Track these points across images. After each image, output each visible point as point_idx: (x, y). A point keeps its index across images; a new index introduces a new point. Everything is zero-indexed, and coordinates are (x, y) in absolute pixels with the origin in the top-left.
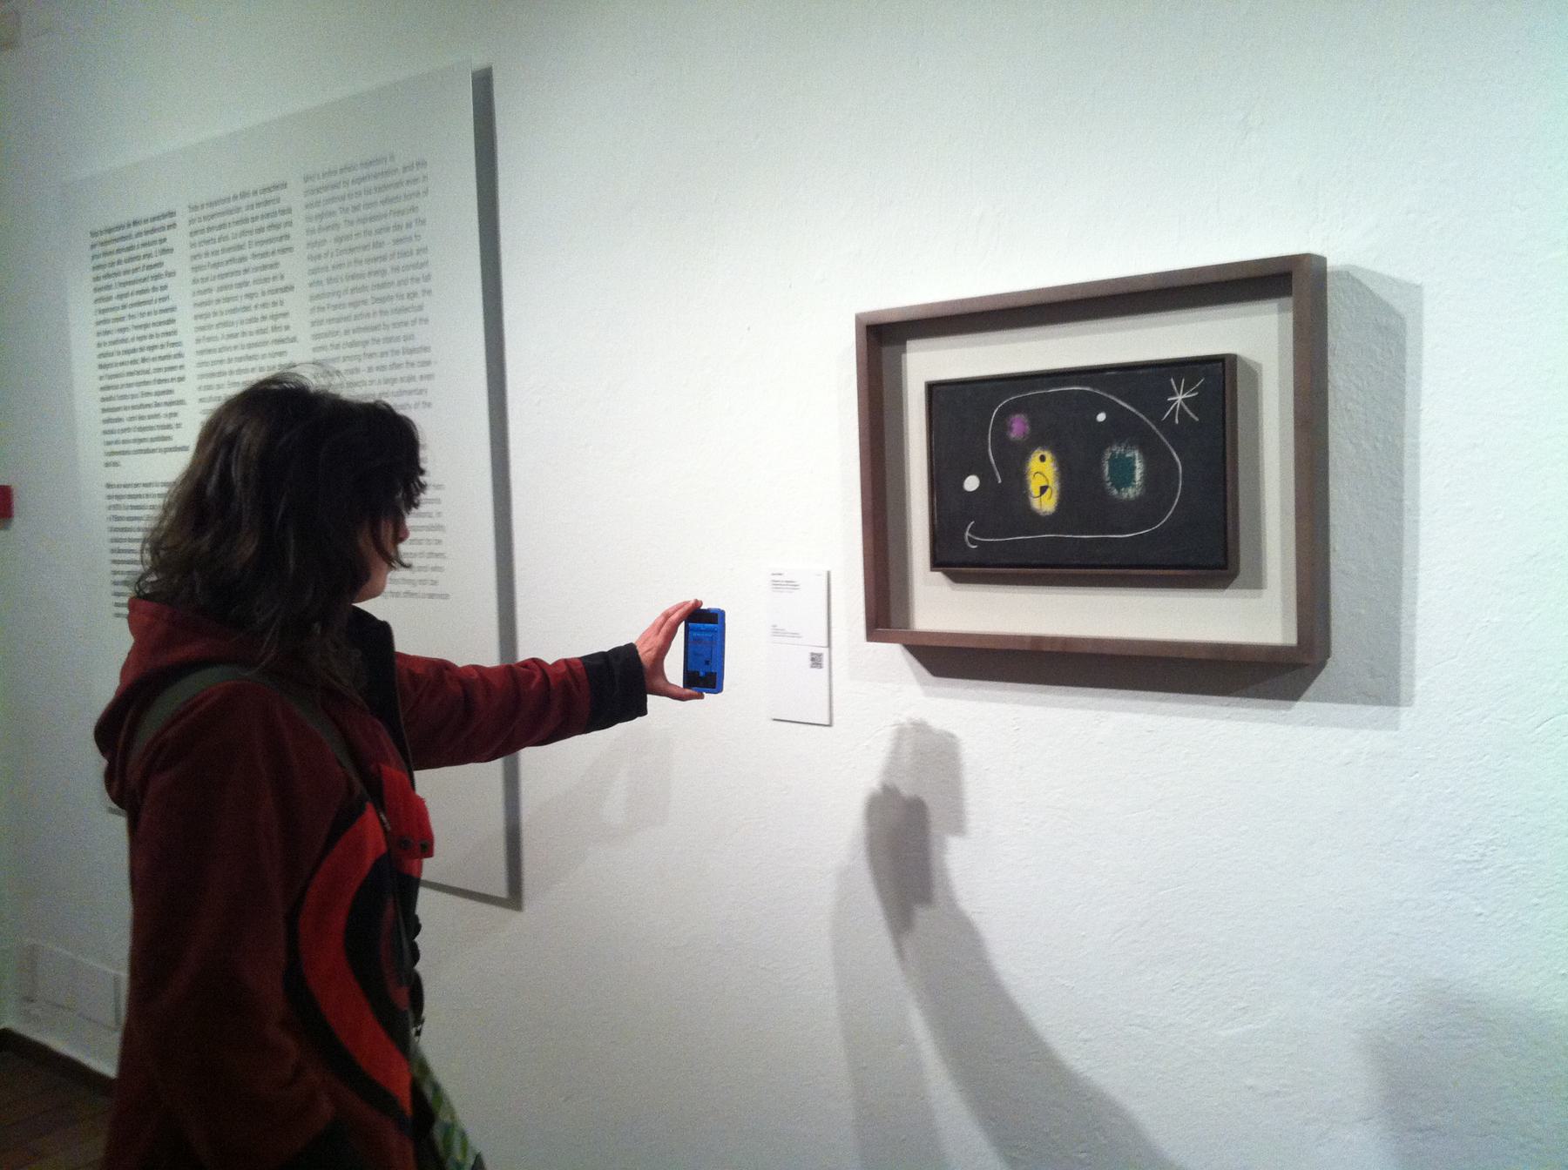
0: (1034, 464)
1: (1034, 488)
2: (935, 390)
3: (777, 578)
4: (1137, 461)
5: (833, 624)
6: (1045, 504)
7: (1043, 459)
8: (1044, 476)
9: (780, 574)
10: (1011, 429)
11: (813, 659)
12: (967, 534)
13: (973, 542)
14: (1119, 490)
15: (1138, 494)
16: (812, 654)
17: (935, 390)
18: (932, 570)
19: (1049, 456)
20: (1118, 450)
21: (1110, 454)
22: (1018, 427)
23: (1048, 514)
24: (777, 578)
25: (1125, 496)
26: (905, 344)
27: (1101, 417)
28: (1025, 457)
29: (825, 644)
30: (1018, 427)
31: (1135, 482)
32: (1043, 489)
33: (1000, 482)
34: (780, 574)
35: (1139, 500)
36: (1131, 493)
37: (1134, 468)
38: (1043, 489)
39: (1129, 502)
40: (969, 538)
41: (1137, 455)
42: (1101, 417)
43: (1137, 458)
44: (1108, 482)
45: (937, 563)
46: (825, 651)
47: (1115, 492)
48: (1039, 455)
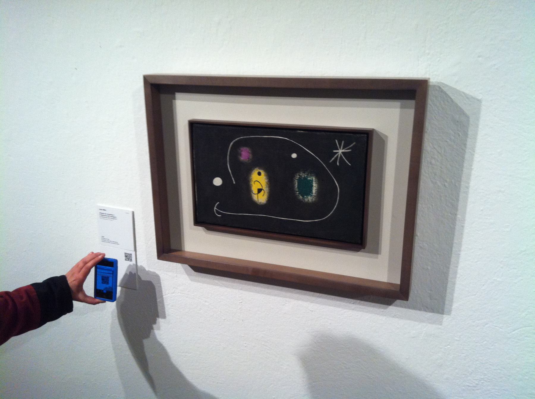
0: (254, 176)
1: (254, 189)
2: (193, 125)
3: (103, 212)
4: (314, 182)
5: (137, 239)
7: (259, 174)
8: (260, 183)
9: (104, 210)
10: (241, 155)
11: (126, 256)
14: (303, 197)
15: (314, 200)
16: (125, 253)
17: (193, 125)
19: (263, 173)
20: (303, 175)
21: (298, 176)
22: (245, 155)
23: (262, 204)
24: (103, 212)
25: (306, 200)
26: (174, 94)
27: (294, 156)
28: (249, 172)
30: (245, 155)
31: (312, 193)
32: (260, 191)
34: (104, 210)
35: (313, 204)
36: (310, 199)
37: (312, 186)
38: (260, 191)
39: (308, 204)
40: (216, 210)
41: (314, 179)
42: (294, 156)
43: (314, 180)
44: (297, 191)
47: (301, 197)
48: (258, 171)
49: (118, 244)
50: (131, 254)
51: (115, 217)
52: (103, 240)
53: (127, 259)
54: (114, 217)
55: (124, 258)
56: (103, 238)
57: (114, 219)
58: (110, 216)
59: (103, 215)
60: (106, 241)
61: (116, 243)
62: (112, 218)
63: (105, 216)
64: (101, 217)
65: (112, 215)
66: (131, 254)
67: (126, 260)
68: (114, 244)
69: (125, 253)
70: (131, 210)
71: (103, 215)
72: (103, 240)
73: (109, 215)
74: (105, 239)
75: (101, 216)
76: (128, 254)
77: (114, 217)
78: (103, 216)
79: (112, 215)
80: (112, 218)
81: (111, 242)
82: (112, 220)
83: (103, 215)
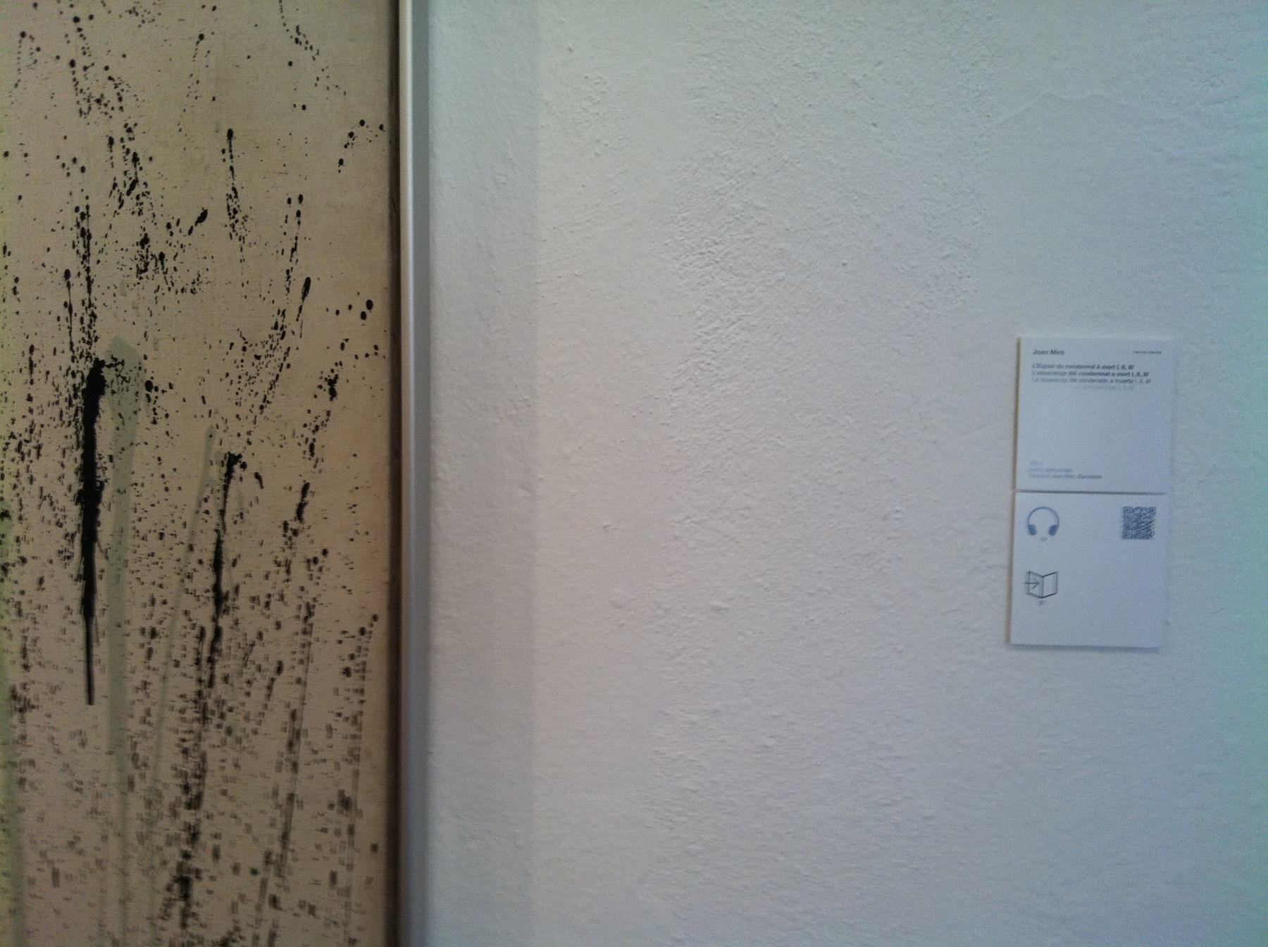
9: (1053, 352)
16: (1126, 510)
34: (1053, 352)
55: (1118, 528)
58: (1082, 370)
59: (1049, 373)
63: (1058, 377)
66: (1152, 510)
69: (1126, 510)
75: (1041, 377)
83: (1049, 373)
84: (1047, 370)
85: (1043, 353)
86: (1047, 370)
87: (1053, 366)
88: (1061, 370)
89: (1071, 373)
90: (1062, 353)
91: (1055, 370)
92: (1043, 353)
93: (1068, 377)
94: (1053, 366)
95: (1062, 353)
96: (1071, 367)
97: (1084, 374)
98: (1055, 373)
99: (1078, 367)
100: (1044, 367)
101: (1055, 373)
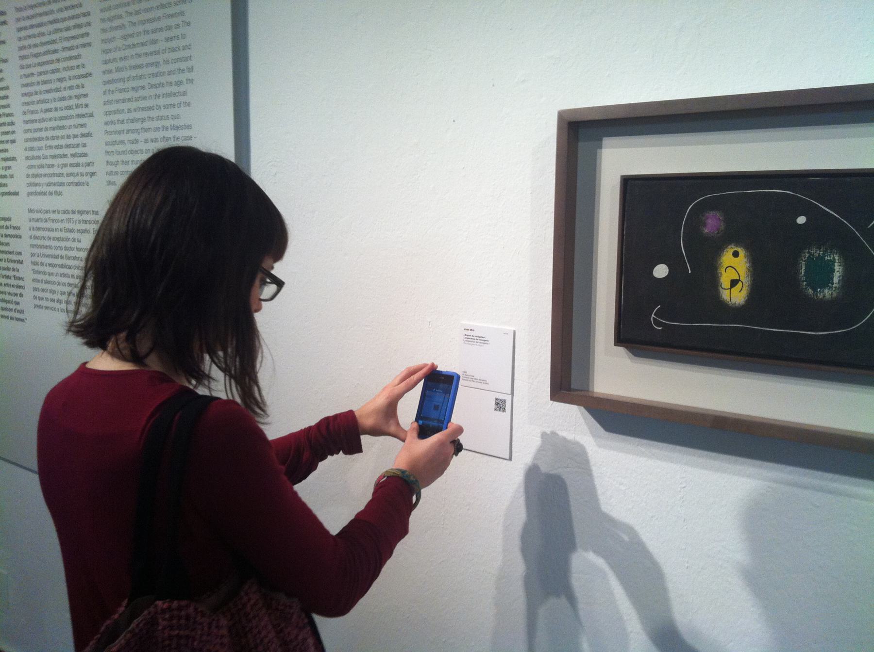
0: (727, 258)
1: (725, 279)
2: (628, 183)
3: (469, 333)
4: (836, 264)
6: (737, 296)
7: (736, 254)
8: (736, 270)
9: (471, 330)
10: (705, 225)
11: (497, 404)
12: (653, 316)
13: (658, 323)
14: (814, 290)
15: (835, 294)
16: (496, 399)
17: (628, 183)
18: (615, 345)
19: (742, 252)
20: (816, 252)
21: (807, 255)
22: (712, 223)
23: (737, 305)
24: (469, 333)
25: (820, 296)
26: (601, 140)
27: (801, 220)
28: (718, 250)
29: (510, 392)
30: (712, 223)
31: (833, 283)
32: (734, 283)
33: (690, 272)
34: (471, 330)
35: (833, 302)
36: (827, 293)
37: (833, 271)
38: (734, 283)
39: (823, 302)
41: (837, 258)
42: (801, 220)
43: (837, 261)
44: (803, 281)
45: (620, 339)
46: (508, 398)
47: (810, 291)
48: (732, 251)
49: (486, 383)
50: (505, 401)
51: (487, 341)
52: (464, 377)
53: (498, 409)
54: (486, 341)
55: (494, 406)
56: (465, 374)
57: (485, 343)
59: (469, 338)
60: (469, 379)
61: (485, 382)
62: (483, 343)
63: (472, 340)
64: (466, 342)
65: (482, 337)
66: (505, 401)
67: (496, 409)
68: (481, 383)
69: (496, 399)
70: (513, 329)
71: (467, 337)
72: (464, 377)
73: (478, 338)
74: (467, 376)
75: (466, 339)
76: (501, 400)
77: (486, 341)
78: (468, 340)
79: (482, 337)
80: (483, 343)
81: (476, 380)
82: (482, 346)
83: (469, 338)
84: (469, 337)
85: (468, 330)
86: (469, 337)
87: (470, 336)
88: (472, 338)
89: (477, 339)
90: (474, 330)
91: (471, 337)
92: (468, 330)
93: (475, 341)
94: (470, 336)
95: (474, 330)
96: (476, 337)
97: (481, 340)
98: (471, 339)
99: (479, 337)
100: (467, 336)
101: (471, 339)
